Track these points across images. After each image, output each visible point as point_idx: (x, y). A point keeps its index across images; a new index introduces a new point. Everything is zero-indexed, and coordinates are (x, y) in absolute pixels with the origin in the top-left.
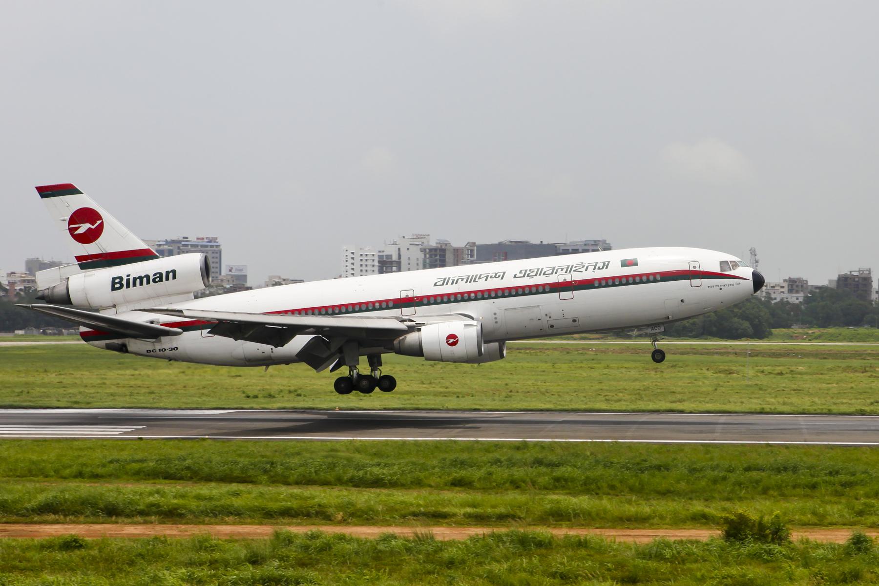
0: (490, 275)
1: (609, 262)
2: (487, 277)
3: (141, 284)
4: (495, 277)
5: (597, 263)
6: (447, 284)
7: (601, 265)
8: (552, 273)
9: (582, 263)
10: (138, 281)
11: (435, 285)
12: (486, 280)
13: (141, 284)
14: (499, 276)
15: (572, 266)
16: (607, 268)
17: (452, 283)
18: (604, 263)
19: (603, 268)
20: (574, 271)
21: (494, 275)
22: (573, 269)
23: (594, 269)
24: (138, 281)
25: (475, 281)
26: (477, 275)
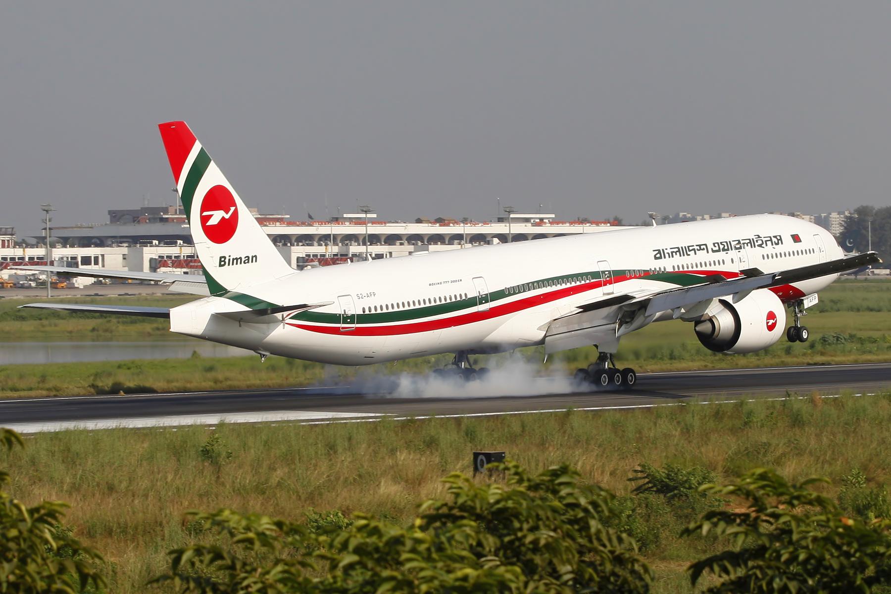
4: (700, 249)
8: (740, 248)
10: (235, 261)
12: (695, 254)
13: (237, 264)
14: (704, 249)
16: (782, 243)
17: (669, 257)
22: (756, 244)
24: (235, 261)
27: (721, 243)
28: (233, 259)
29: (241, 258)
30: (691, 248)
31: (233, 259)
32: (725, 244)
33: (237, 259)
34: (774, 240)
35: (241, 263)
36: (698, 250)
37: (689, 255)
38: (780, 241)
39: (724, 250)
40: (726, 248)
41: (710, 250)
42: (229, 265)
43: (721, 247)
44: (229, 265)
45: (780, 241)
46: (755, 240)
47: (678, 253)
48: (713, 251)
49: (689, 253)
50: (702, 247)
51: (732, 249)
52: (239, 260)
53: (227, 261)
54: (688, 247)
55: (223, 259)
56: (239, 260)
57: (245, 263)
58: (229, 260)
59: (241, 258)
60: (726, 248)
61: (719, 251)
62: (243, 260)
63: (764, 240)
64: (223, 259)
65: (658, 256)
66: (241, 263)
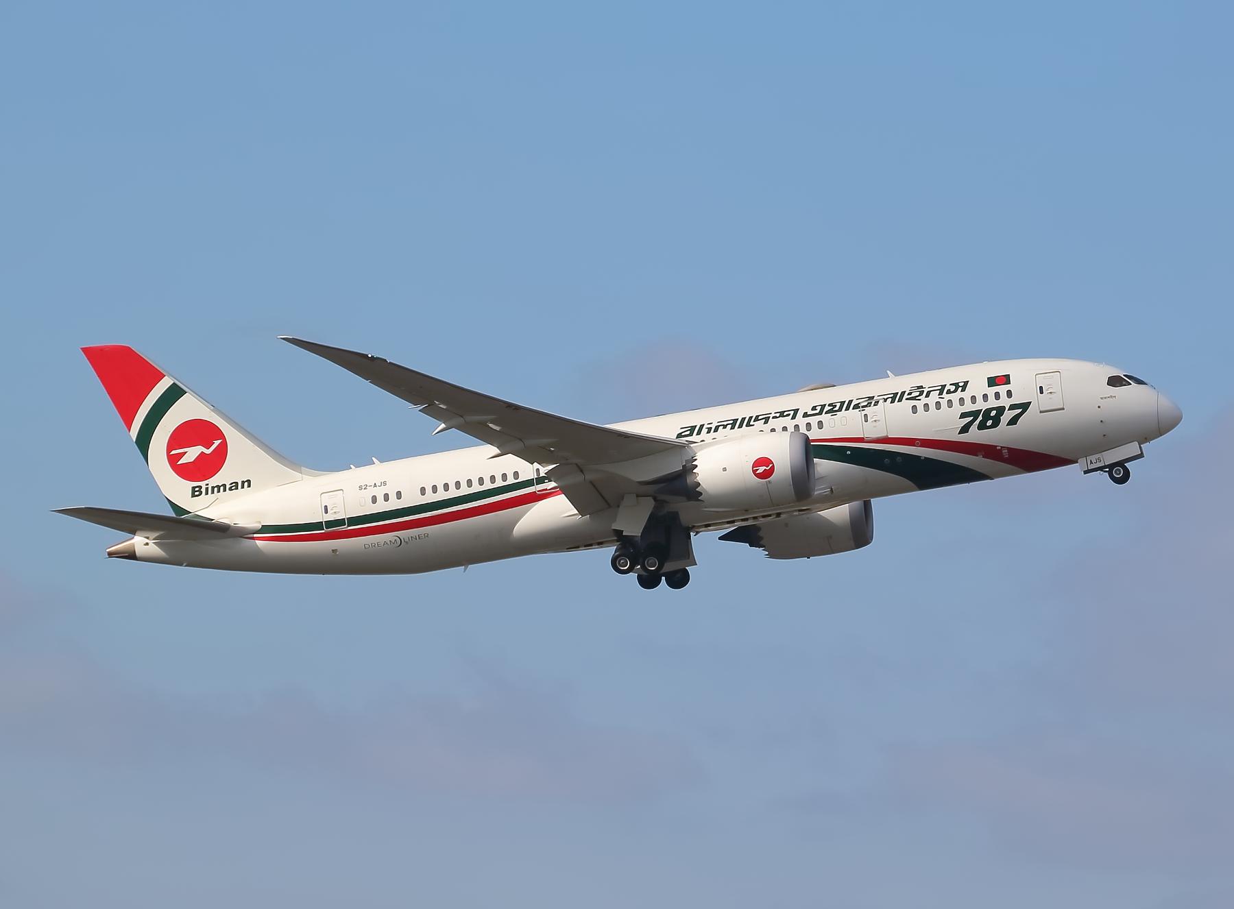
0: (771, 416)
1: (966, 383)
2: (767, 420)
3: (219, 491)
5: (944, 386)
6: (699, 433)
7: (953, 388)
8: (869, 405)
9: (922, 387)
10: (216, 489)
11: (679, 436)
13: (219, 491)
14: (789, 415)
17: (709, 430)
18: (957, 385)
19: (955, 391)
20: (907, 399)
22: (906, 396)
24: (216, 489)
25: (748, 425)
26: (751, 418)
28: (213, 488)
29: (224, 486)
30: (760, 418)
31: (213, 488)
32: (838, 405)
33: (218, 487)
35: (225, 490)
36: (773, 418)
37: (753, 425)
38: (960, 389)
40: (837, 408)
41: (800, 414)
42: (207, 493)
44: (207, 493)
45: (960, 389)
46: (906, 393)
47: (729, 426)
48: (806, 415)
50: (785, 414)
51: (847, 409)
52: (222, 488)
53: (203, 490)
55: (197, 489)
56: (222, 488)
57: (230, 489)
58: (207, 489)
59: (224, 486)
60: (837, 408)
61: (820, 413)
63: (926, 391)
64: (197, 489)
65: (688, 433)
66: (225, 490)
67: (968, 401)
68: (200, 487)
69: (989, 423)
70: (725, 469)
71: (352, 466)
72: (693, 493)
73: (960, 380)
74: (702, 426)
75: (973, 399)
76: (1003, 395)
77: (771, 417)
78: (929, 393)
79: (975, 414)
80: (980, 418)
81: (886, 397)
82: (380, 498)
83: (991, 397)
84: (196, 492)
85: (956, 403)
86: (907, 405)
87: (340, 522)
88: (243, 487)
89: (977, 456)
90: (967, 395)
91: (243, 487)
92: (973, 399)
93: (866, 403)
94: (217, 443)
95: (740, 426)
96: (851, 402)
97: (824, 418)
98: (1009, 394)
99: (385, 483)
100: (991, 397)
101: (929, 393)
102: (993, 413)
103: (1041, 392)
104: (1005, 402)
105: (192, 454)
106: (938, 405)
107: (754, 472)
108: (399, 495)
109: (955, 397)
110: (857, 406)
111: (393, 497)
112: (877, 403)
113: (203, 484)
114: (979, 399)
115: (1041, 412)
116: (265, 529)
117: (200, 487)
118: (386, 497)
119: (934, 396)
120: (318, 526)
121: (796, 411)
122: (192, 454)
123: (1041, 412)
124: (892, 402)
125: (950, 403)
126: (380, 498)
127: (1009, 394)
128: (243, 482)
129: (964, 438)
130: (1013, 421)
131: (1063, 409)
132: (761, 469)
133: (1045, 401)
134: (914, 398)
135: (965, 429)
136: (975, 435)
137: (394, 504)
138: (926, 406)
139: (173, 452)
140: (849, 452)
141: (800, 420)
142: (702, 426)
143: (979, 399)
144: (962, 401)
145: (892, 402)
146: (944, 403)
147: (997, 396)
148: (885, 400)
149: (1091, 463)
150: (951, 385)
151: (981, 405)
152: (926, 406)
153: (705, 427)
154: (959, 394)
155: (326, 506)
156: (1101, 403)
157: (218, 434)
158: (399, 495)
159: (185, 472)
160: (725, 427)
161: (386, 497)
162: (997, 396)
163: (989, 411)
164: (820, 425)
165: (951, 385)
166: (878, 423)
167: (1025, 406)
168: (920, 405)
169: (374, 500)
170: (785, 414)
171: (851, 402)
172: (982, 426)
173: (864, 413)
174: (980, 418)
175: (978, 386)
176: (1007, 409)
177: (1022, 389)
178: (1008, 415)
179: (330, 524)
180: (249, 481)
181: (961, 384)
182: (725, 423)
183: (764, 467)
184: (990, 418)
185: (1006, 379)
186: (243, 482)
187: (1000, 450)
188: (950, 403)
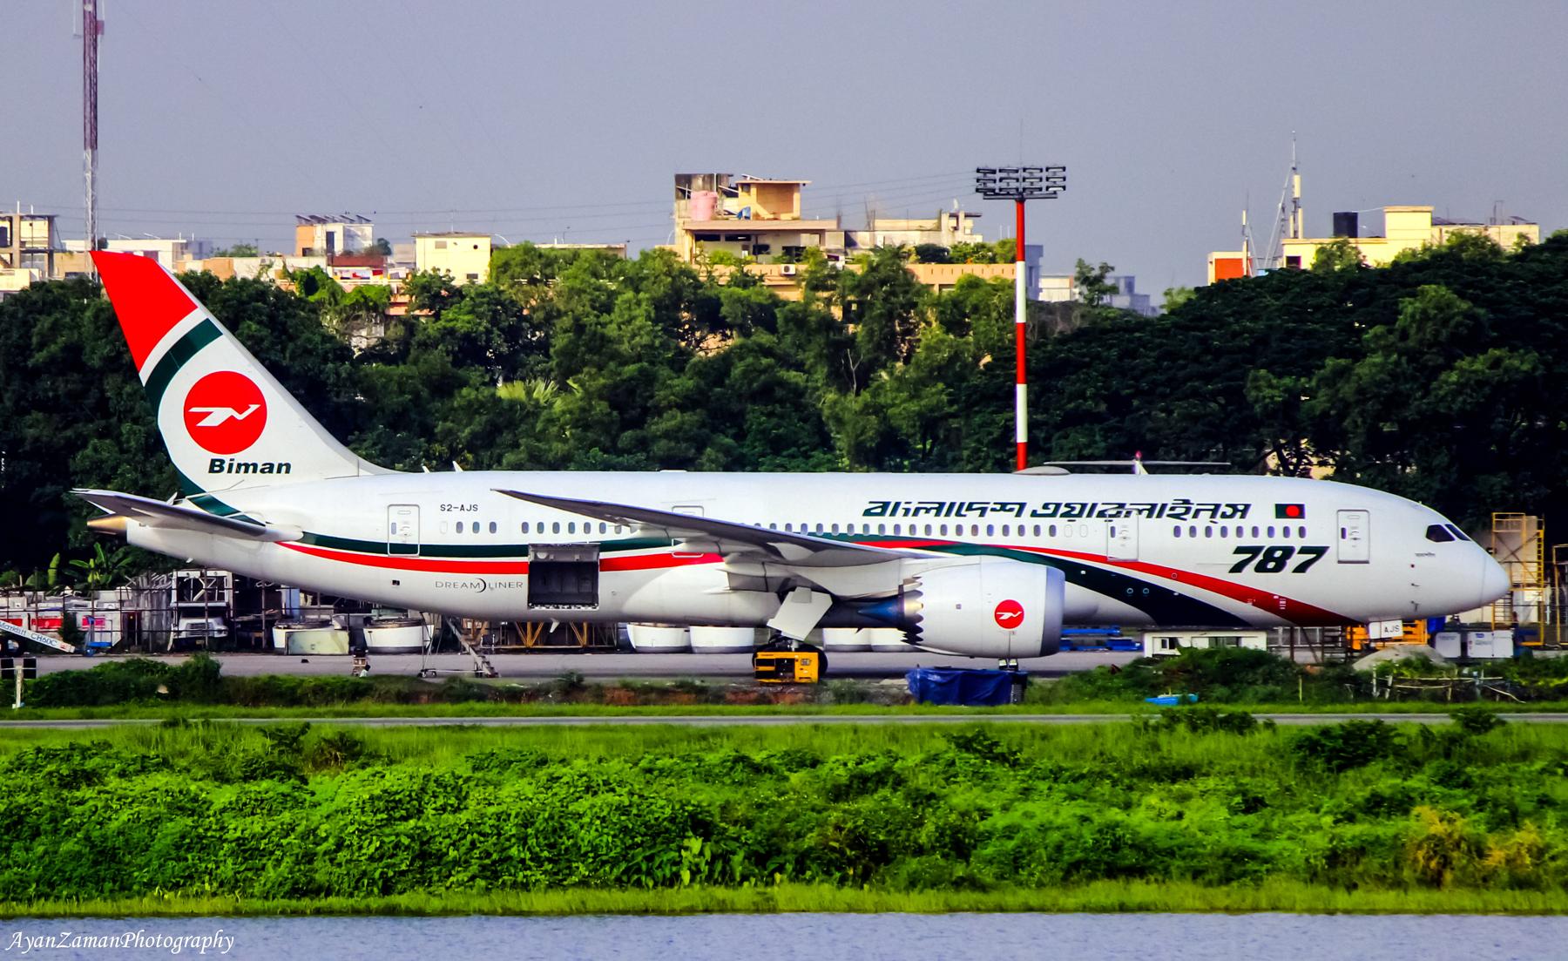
0: (991, 506)
1: (1247, 507)
2: (983, 511)
3: (246, 471)
5: (1217, 506)
6: (893, 513)
7: (1229, 511)
8: (1118, 515)
9: (1186, 502)
10: (243, 468)
11: (867, 513)
12: (982, 515)
13: (246, 471)
14: (1011, 510)
15: (1164, 506)
16: (1243, 517)
17: (907, 511)
18: (1234, 507)
19: (1232, 516)
20: (1169, 516)
21: (998, 507)
22: (1167, 511)
23: (1213, 516)
24: (243, 468)
25: (958, 514)
26: (962, 504)
27: (1067, 505)
28: (239, 465)
29: (255, 465)
30: (975, 506)
31: (239, 465)
32: (1078, 507)
33: (247, 466)
34: (1223, 509)
35: (255, 471)
36: (993, 510)
38: (1239, 514)
39: (1062, 516)
41: (1027, 511)
42: (230, 471)
43: (1063, 509)
44: (230, 471)
45: (1239, 514)
47: (934, 511)
48: (1034, 514)
49: (963, 512)
50: (1008, 507)
51: (1089, 515)
53: (226, 466)
54: (971, 504)
57: (262, 471)
58: (231, 466)
59: (255, 465)
61: (1053, 515)
62: (260, 467)
63: (1194, 508)
65: (879, 510)
66: (255, 471)
67: (1247, 532)
68: (222, 462)
69: (1271, 565)
70: (959, 607)
71: (425, 468)
72: (910, 628)
73: (1239, 500)
74: (897, 504)
75: (1255, 531)
76: (1294, 532)
77: (988, 511)
78: (1198, 511)
79: (1254, 551)
80: (1260, 557)
81: (1141, 507)
82: (468, 528)
83: (1279, 532)
84: (216, 467)
85: (1232, 532)
86: (1168, 523)
87: (411, 549)
88: (279, 471)
89: (1246, 602)
90: (1247, 524)
91: (279, 471)
92: (1255, 531)
93: (1114, 512)
94: (253, 407)
95: (948, 514)
96: (1094, 506)
97: (1058, 521)
98: (1302, 532)
99: (474, 507)
100: (1279, 532)
101: (1198, 511)
102: (1278, 554)
103: (1343, 536)
104: (1295, 542)
105: (218, 416)
106: (1208, 531)
107: (997, 617)
108: (493, 527)
109: (1231, 524)
110: (1101, 514)
111: (484, 527)
112: (1128, 514)
113: (227, 458)
114: (1263, 532)
115: (1340, 562)
116: (307, 537)
117: (222, 462)
118: (476, 527)
119: (1205, 516)
120: (380, 547)
121: (1022, 506)
122: (218, 416)
123: (1340, 562)
124: (1149, 516)
125: (1224, 531)
126: (468, 528)
127: (1302, 532)
128: (280, 466)
129: (1236, 579)
130: (1302, 568)
131: (1367, 562)
132: (1006, 616)
133: (1347, 549)
134: (1177, 516)
135: (1238, 568)
136: (1250, 578)
137: (484, 539)
138: (1193, 531)
139: (194, 410)
140: (1083, 572)
141: (1026, 520)
142: (897, 504)
143: (1263, 532)
144: (1239, 531)
145: (1149, 516)
146: (1216, 530)
147: (1286, 532)
148: (1140, 512)
149: (1386, 630)
150: (1228, 505)
151: (1264, 541)
152: (1193, 531)
153: (903, 505)
154: (1236, 521)
155: (394, 524)
156: (1417, 561)
157: (258, 397)
158: (493, 527)
159: (205, 438)
160: (928, 511)
161: (476, 527)
162: (1286, 532)
163: (1272, 550)
164: (1052, 530)
165: (1228, 505)
166: (1124, 542)
167: (1319, 552)
168: (1185, 526)
169: (460, 526)
170: (1008, 507)
171: (1094, 506)
172: (1261, 568)
173: (1111, 524)
174: (1260, 557)
175: (1263, 515)
176: (1297, 550)
177: (1318, 528)
178: (1296, 559)
179: (397, 548)
180: (288, 466)
181: (1241, 508)
182: (929, 506)
183: (1009, 613)
184: (1273, 560)
185: (1297, 511)
186: (280, 466)
187: (1278, 600)
188: (1224, 531)
